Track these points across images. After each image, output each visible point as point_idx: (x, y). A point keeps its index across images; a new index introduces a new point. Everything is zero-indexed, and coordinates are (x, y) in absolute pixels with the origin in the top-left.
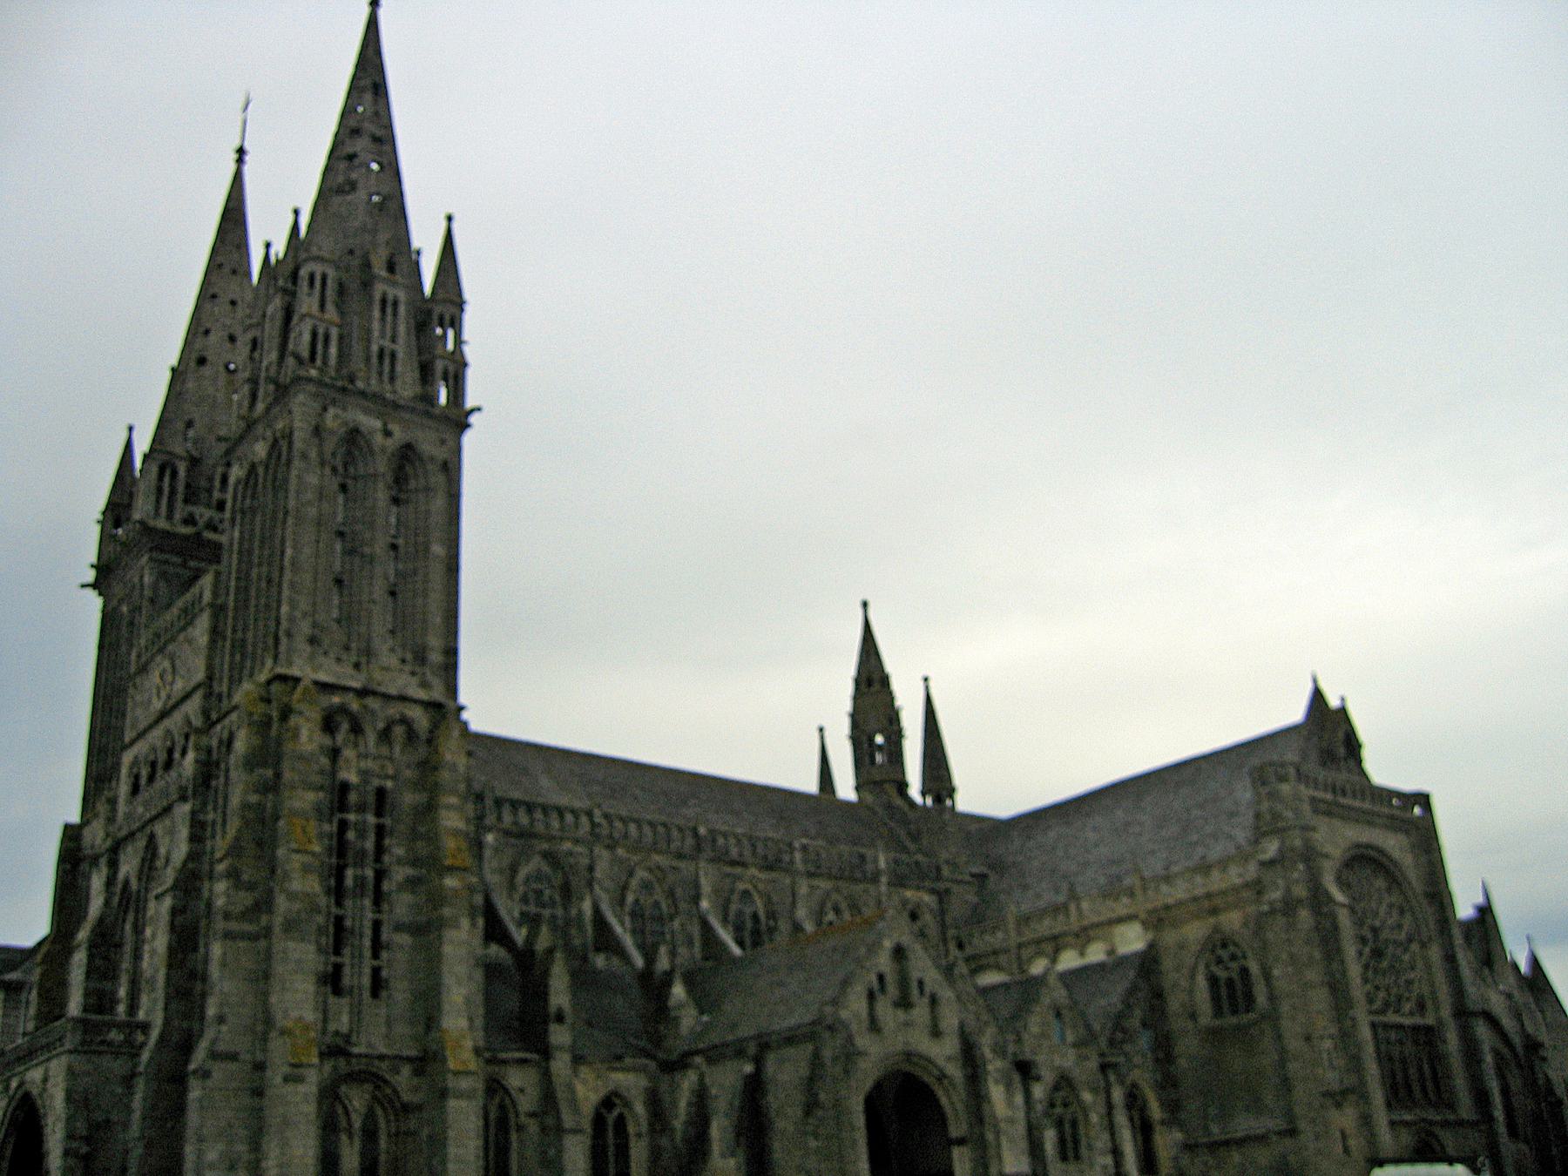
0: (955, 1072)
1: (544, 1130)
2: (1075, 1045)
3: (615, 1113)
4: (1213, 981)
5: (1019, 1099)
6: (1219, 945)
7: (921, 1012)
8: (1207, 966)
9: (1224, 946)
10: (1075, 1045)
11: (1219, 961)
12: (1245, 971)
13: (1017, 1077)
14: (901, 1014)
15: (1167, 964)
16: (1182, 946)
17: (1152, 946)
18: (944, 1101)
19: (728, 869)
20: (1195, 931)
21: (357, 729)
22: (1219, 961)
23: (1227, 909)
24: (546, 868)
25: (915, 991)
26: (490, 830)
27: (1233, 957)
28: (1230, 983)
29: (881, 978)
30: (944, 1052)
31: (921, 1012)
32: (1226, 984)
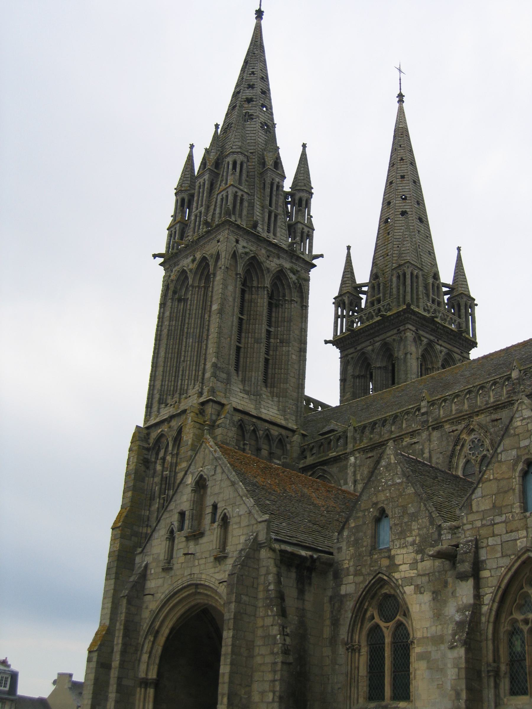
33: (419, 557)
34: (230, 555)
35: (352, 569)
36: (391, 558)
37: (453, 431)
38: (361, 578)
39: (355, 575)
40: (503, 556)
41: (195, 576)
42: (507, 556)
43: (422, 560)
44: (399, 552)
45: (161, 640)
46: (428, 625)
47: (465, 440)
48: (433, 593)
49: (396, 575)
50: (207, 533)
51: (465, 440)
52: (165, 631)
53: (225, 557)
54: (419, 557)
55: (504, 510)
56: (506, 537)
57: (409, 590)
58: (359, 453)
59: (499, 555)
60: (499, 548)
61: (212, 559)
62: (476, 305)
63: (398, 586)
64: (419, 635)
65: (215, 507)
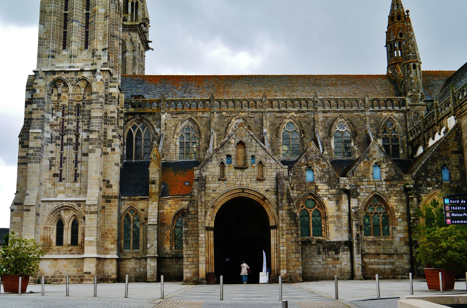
0: (271, 197)
2: (384, 180)
5: (345, 206)
7: (253, 171)
10: (384, 180)
13: (344, 196)
14: (239, 172)
18: (267, 209)
19: (278, 115)
21: (66, 85)
24: (191, 124)
25: (249, 161)
26: (163, 113)
29: (229, 156)
30: (261, 187)
31: (253, 171)
33: (329, 188)
34: (267, 179)
35: (295, 188)
36: (317, 187)
37: (227, 117)
38: (301, 192)
39: (297, 190)
40: (366, 192)
41: (244, 185)
42: (367, 192)
43: (331, 189)
44: (320, 184)
45: (217, 211)
46: (334, 212)
47: (233, 122)
48: (336, 201)
49: (319, 193)
50: (250, 168)
51: (233, 122)
52: (219, 207)
53: (264, 180)
54: (329, 188)
55: (367, 178)
56: (368, 186)
57: (325, 199)
58: (168, 114)
59: (365, 192)
60: (365, 189)
61: (255, 179)
62: (150, 26)
63: (320, 197)
64: (330, 215)
65: (253, 157)
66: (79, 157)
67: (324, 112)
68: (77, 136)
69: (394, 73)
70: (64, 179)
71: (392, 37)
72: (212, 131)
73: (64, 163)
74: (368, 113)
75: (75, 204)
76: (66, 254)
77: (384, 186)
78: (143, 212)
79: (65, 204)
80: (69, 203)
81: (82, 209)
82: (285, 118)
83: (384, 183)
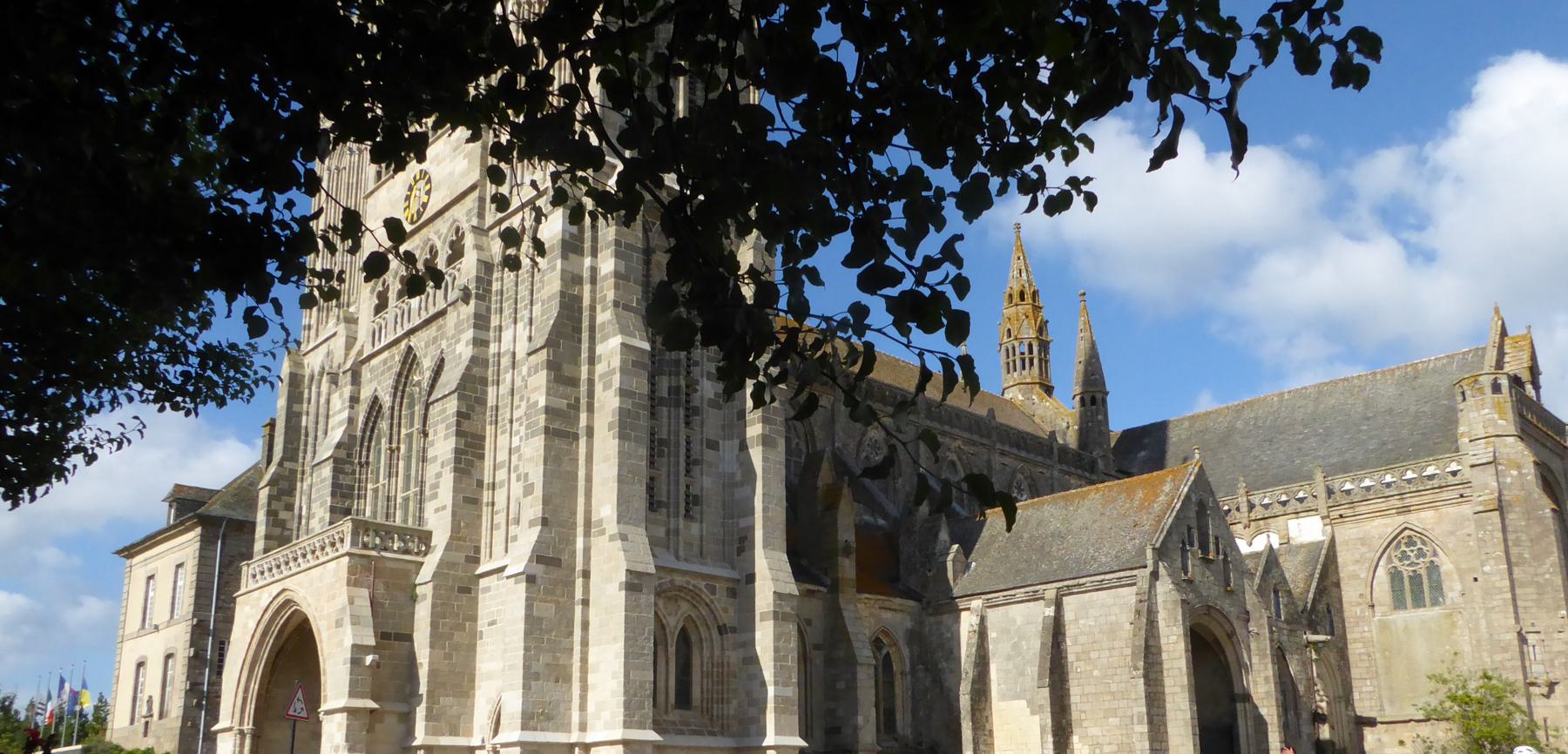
1: (829, 662)
2: (1287, 621)
3: (884, 652)
4: (1395, 576)
6: (1405, 540)
8: (1390, 560)
9: (1410, 542)
11: (1404, 557)
12: (1433, 568)
15: (1343, 556)
16: (1363, 541)
17: (1333, 541)
20: (1382, 527)
22: (1404, 557)
23: (1422, 507)
27: (1421, 554)
28: (1416, 579)
32: (1410, 577)
66: (696, 447)
67: (1003, 453)
68: (692, 386)
69: (1027, 402)
70: (660, 505)
71: (1026, 331)
72: (836, 445)
73: (661, 455)
74: (1056, 473)
75: (702, 584)
76: (681, 733)
77: (1285, 632)
78: (808, 628)
79: (679, 580)
80: (687, 578)
81: (719, 601)
82: (949, 449)
83: (1285, 626)
